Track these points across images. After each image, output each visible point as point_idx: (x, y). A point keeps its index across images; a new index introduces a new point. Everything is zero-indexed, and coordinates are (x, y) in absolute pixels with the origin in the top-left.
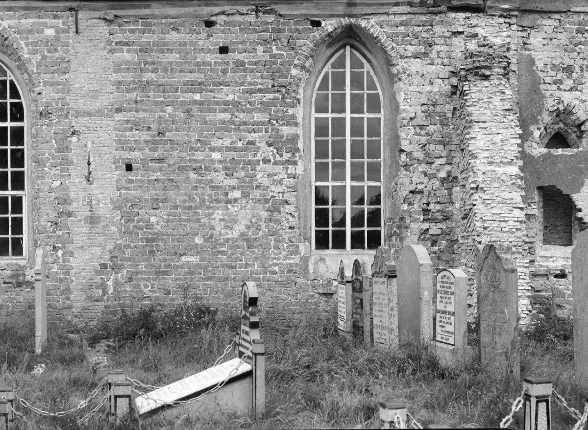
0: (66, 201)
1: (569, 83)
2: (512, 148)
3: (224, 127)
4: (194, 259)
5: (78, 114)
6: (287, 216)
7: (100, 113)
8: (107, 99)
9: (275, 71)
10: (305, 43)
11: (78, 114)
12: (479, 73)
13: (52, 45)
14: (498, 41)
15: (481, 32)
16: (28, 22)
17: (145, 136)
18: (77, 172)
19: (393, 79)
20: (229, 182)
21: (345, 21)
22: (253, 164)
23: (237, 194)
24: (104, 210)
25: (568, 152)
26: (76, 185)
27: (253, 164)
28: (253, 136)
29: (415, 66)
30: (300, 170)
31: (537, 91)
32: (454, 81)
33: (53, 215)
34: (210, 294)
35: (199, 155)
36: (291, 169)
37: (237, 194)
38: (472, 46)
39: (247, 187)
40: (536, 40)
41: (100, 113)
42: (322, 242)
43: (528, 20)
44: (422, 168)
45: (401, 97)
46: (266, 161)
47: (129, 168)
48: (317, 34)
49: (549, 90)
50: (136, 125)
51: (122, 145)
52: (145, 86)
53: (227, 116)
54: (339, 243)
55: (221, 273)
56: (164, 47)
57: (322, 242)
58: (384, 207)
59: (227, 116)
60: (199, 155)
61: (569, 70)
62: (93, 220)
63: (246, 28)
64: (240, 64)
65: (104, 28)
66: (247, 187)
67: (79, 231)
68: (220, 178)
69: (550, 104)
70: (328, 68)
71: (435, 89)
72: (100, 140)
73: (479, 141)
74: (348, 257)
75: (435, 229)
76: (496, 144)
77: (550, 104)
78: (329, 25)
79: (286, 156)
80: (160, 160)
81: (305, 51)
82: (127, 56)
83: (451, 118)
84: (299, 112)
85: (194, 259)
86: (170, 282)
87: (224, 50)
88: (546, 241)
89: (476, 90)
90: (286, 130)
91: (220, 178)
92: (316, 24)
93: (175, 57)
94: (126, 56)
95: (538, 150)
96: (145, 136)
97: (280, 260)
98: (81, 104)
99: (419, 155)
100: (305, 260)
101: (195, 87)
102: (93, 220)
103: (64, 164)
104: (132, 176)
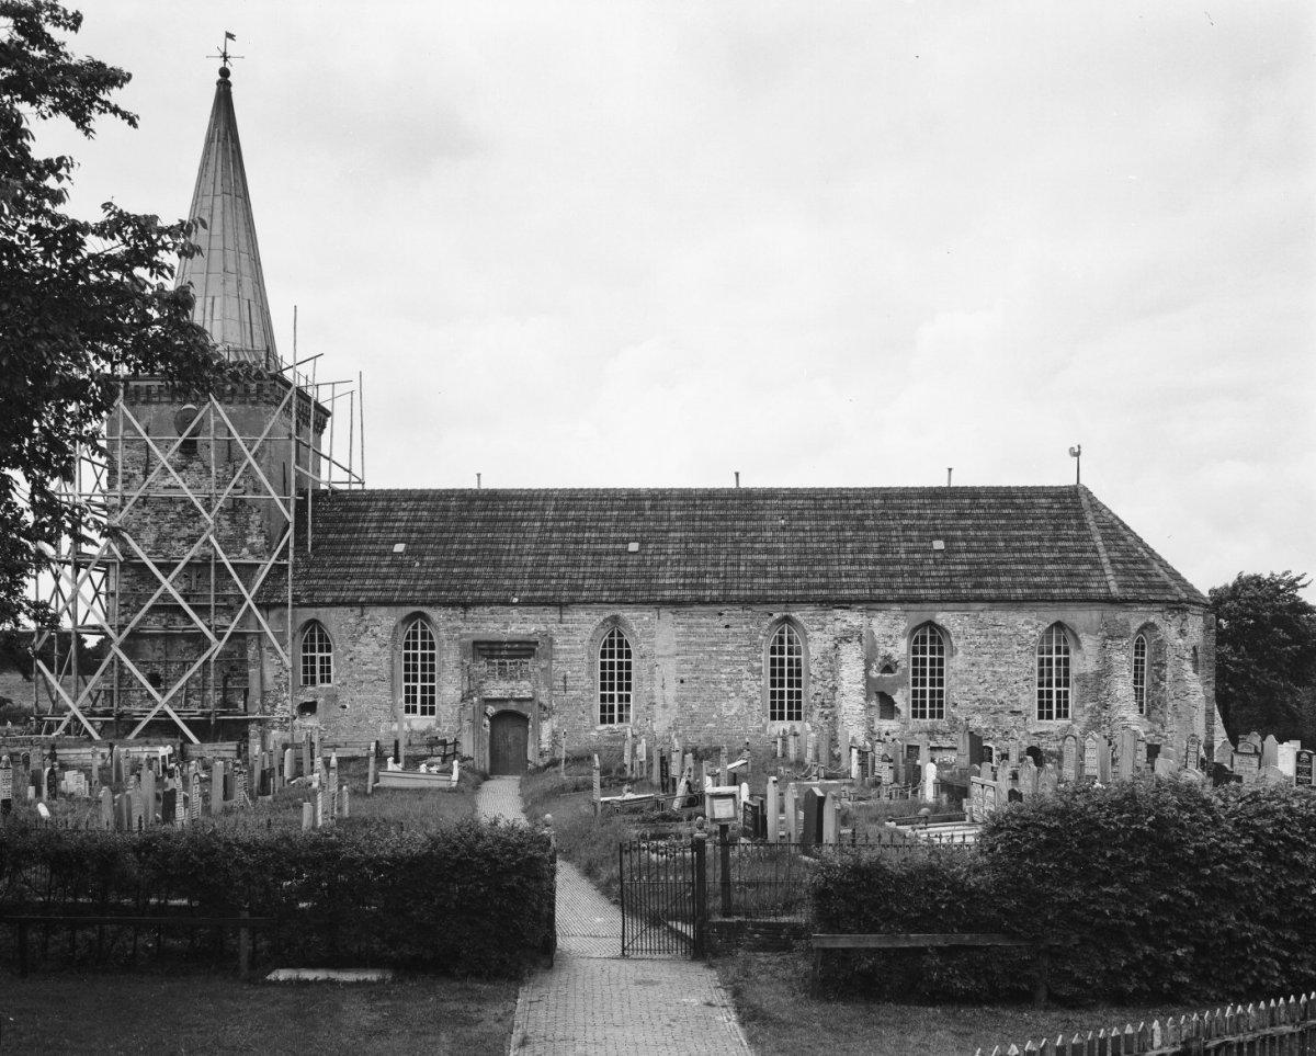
0: (652, 697)
1: (890, 643)
2: (861, 675)
3: (727, 663)
4: (712, 725)
5: (659, 657)
6: (757, 705)
7: (669, 656)
8: (673, 649)
9: (751, 637)
10: (766, 624)
11: (659, 657)
12: (846, 640)
13: (647, 624)
14: (856, 624)
15: (849, 619)
16: (636, 614)
17: (690, 667)
18: (658, 684)
19: (807, 640)
20: (729, 689)
21: (784, 614)
22: (741, 680)
23: (733, 694)
24: (670, 702)
25: (890, 675)
26: (658, 691)
27: (741, 680)
28: (742, 667)
29: (818, 635)
30: (763, 683)
31: (875, 647)
32: (836, 642)
33: (646, 704)
34: (718, 740)
35: (715, 676)
36: (759, 683)
37: (733, 694)
38: (844, 626)
39: (738, 691)
40: (875, 622)
41: (669, 656)
42: (773, 717)
43: (871, 613)
44: (821, 682)
45: (811, 649)
46: (747, 679)
47: (682, 682)
48: (771, 620)
49: (881, 646)
50: (686, 662)
51: (679, 671)
52: (690, 644)
53: (729, 658)
54: (781, 718)
55: (724, 732)
56: (699, 625)
57: (773, 717)
58: (803, 700)
59: (729, 658)
60: (715, 676)
61: (890, 637)
62: (665, 706)
63: (737, 616)
64: (735, 634)
65: (671, 616)
66: (738, 691)
67: (659, 712)
68: (725, 687)
69: (881, 653)
70: (777, 634)
71: (827, 645)
72: (669, 669)
73: (845, 672)
74: (786, 725)
75: (827, 712)
76: (852, 673)
77: (881, 653)
78: (777, 616)
79: (757, 677)
80: (697, 678)
81: (766, 627)
82: (681, 629)
83: (832, 661)
84: (763, 656)
85: (712, 725)
86: (701, 736)
87: (727, 627)
88: (881, 717)
89: (844, 648)
90: (756, 665)
91: (725, 687)
92: (771, 615)
93: (704, 630)
94: (681, 629)
95: (875, 674)
96: (690, 667)
97: (754, 726)
98: (660, 653)
99: (820, 677)
100: (765, 726)
101: (714, 644)
102: (665, 706)
103: (652, 680)
104: (682, 685)
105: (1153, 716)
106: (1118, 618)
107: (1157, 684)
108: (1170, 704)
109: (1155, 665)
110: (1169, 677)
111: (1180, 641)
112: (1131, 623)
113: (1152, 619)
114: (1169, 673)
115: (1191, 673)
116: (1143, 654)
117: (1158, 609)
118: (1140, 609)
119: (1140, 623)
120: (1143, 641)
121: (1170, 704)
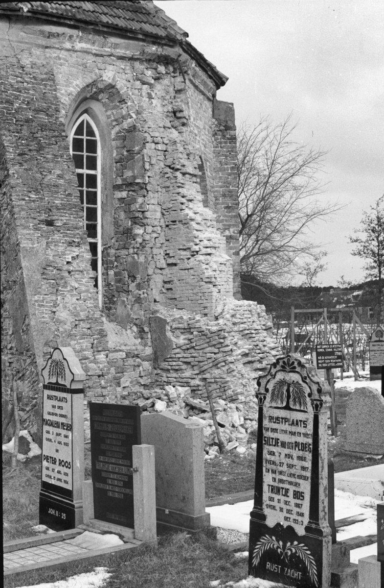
105: (120, 310)
106: (26, 61)
107: (128, 233)
108: (157, 280)
109: (117, 188)
110: (154, 214)
111: (174, 134)
112: (60, 78)
113: (108, 75)
114: (152, 206)
115: (199, 207)
116: (92, 164)
117: (120, 52)
118: (79, 46)
119: (78, 83)
120: (91, 133)
121: (157, 280)
